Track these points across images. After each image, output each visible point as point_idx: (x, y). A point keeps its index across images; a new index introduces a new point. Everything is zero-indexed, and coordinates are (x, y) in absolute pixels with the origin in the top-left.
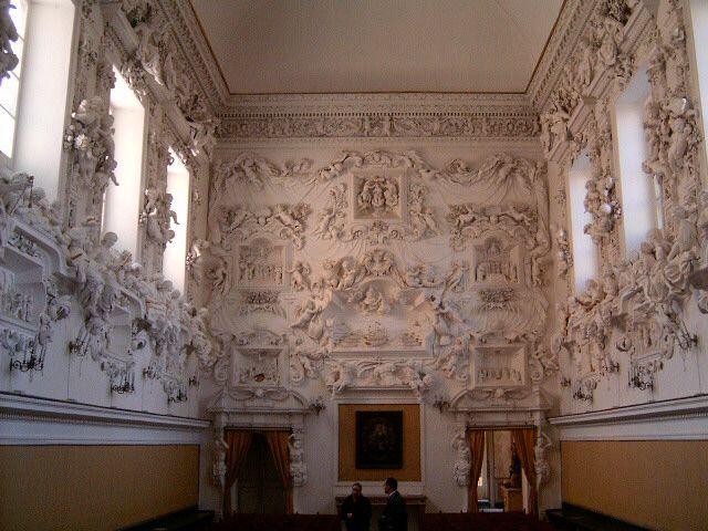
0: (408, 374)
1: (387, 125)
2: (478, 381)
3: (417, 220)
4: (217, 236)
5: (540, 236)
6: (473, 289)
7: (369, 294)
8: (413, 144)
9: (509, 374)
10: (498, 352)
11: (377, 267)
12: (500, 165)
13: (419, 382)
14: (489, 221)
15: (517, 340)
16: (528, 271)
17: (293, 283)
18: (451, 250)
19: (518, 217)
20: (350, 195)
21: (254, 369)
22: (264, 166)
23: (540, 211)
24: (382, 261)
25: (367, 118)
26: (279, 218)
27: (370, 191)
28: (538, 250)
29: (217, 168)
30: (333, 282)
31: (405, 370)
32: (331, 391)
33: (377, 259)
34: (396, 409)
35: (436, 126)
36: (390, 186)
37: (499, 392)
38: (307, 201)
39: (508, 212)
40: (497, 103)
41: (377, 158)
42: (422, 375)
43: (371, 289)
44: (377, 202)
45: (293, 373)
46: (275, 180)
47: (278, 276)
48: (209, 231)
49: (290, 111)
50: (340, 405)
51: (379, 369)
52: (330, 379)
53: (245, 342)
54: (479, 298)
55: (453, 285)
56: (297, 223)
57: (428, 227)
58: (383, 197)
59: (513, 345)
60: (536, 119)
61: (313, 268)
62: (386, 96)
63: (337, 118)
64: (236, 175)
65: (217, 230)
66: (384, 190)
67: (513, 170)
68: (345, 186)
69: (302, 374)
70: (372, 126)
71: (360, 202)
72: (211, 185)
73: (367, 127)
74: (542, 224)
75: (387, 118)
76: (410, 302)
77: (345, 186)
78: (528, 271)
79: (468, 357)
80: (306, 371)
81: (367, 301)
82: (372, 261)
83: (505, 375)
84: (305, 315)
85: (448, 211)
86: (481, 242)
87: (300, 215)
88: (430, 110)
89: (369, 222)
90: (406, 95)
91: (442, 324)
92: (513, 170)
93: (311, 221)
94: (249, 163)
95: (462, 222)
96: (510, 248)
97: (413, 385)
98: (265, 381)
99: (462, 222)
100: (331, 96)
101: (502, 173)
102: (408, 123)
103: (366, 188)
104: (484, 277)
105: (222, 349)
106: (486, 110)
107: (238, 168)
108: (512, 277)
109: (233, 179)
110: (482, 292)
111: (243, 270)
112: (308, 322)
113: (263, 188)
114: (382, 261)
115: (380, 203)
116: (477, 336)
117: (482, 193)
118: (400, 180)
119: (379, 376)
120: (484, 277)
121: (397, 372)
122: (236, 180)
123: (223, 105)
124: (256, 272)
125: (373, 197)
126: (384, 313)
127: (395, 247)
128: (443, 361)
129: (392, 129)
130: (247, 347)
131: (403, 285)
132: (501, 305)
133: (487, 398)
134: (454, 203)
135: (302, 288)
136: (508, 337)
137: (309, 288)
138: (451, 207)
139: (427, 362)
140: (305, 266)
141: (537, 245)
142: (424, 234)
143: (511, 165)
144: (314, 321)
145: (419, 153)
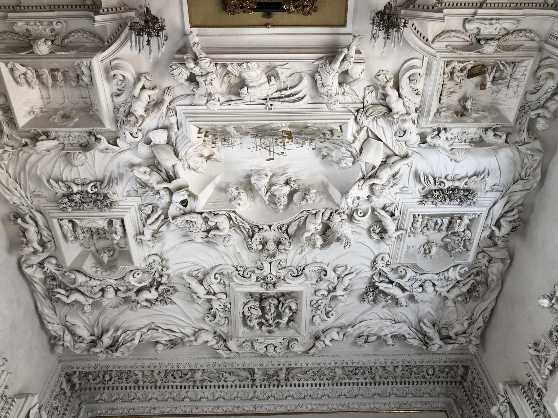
0: (216, 83)
1: (258, 375)
2: (90, 68)
3: (216, 288)
4: (495, 269)
5: (38, 275)
6: (127, 210)
7: (285, 200)
8: (229, 360)
9: (39, 76)
10: (65, 117)
11: (271, 235)
12: (113, 346)
13: (197, 71)
14: (117, 290)
15: (35, 139)
16: (45, 233)
17: (397, 214)
18: (165, 256)
19: (76, 296)
20: (305, 313)
21: (483, 86)
22: (416, 343)
23: (47, 302)
24: (264, 243)
25: (283, 382)
26: (404, 290)
27: (279, 315)
28: (36, 260)
29: (475, 341)
30: (337, 218)
31: (224, 88)
32: (358, 52)
33: (271, 246)
34: (229, 18)
35: (198, 376)
36: (254, 322)
37: (43, 48)
38: (366, 306)
39: (91, 301)
40: (127, 405)
41: (271, 348)
42: (192, 79)
43: (282, 207)
44: (271, 305)
45: (419, 86)
46: (403, 329)
47: (418, 225)
48: (503, 277)
49: (372, 389)
50: (344, 25)
51: (270, 90)
52: (356, 70)
53: (490, 133)
54: (115, 198)
55: (156, 216)
56: (382, 286)
57: (201, 282)
58: (262, 309)
59: (40, 130)
60: (77, 387)
61: (365, 233)
62: (259, 410)
63: (318, 382)
64: (452, 334)
65: (492, 277)
66: (262, 316)
67: (94, 344)
68: (312, 322)
69: (404, 82)
70: (276, 374)
71: (294, 307)
72: (487, 323)
73: (283, 375)
74: (39, 288)
75: (258, 383)
76: (222, 189)
77: (312, 322)
78: (45, 233)
79: (116, 109)
80: (397, 86)
81: (286, 190)
82: (278, 243)
83: (46, 74)
84: (385, 174)
85: (174, 298)
86: (123, 268)
87: (373, 292)
88: (207, 393)
89: (282, 288)
90: (236, 411)
91: (167, 160)
92: (94, 344)
93: (361, 285)
94: (435, 348)
95: (153, 290)
96: (82, 257)
97: (206, 64)
98: (469, 67)
99: (153, 290)
100: (325, 409)
101: (107, 340)
102: (233, 378)
103: (285, 319)
104: (111, 222)
105: (532, 122)
106: (140, 393)
107: (446, 339)
108: (67, 226)
109: (458, 328)
110: (110, 206)
111: (468, 228)
112: (384, 164)
113: (420, 321)
114: (264, 243)
115: (266, 304)
116: (104, 144)
117: (136, 319)
118: (242, 330)
119: (269, 80)
120: (111, 222)
121: (240, 85)
122: (453, 328)
123: (455, 400)
124: (446, 225)
125: (277, 307)
126: (258, 172)
127: (247, 259)
128: (158, 104)
129: (252, 372)
130: (486, 124)
131: (233, 215)
132: (75, 189)
133: (66, 37)
134: (169, 306)
135: (384, 208)
136: (56, 142)
137: (373, 210)
138: (172, 302)
139: (187, 101)
140: (376, 237)
141: (41, 264)
142: (206, 274)
143: (97, 350)
144: (374, 167)
145: (218, 356)
